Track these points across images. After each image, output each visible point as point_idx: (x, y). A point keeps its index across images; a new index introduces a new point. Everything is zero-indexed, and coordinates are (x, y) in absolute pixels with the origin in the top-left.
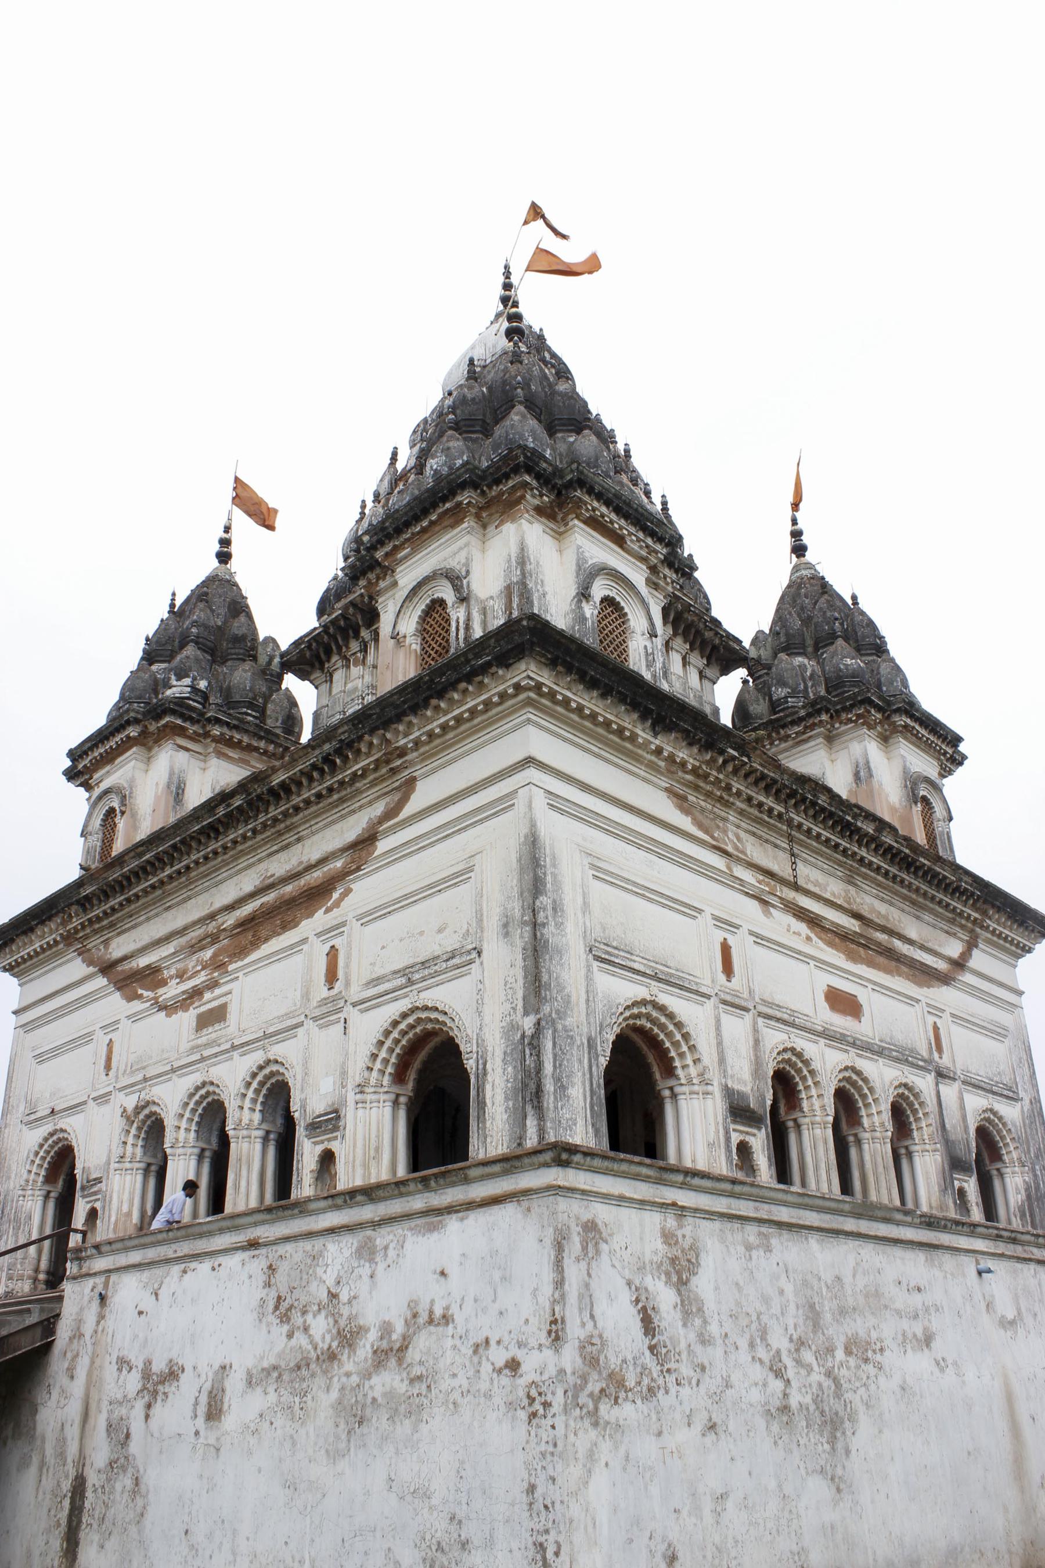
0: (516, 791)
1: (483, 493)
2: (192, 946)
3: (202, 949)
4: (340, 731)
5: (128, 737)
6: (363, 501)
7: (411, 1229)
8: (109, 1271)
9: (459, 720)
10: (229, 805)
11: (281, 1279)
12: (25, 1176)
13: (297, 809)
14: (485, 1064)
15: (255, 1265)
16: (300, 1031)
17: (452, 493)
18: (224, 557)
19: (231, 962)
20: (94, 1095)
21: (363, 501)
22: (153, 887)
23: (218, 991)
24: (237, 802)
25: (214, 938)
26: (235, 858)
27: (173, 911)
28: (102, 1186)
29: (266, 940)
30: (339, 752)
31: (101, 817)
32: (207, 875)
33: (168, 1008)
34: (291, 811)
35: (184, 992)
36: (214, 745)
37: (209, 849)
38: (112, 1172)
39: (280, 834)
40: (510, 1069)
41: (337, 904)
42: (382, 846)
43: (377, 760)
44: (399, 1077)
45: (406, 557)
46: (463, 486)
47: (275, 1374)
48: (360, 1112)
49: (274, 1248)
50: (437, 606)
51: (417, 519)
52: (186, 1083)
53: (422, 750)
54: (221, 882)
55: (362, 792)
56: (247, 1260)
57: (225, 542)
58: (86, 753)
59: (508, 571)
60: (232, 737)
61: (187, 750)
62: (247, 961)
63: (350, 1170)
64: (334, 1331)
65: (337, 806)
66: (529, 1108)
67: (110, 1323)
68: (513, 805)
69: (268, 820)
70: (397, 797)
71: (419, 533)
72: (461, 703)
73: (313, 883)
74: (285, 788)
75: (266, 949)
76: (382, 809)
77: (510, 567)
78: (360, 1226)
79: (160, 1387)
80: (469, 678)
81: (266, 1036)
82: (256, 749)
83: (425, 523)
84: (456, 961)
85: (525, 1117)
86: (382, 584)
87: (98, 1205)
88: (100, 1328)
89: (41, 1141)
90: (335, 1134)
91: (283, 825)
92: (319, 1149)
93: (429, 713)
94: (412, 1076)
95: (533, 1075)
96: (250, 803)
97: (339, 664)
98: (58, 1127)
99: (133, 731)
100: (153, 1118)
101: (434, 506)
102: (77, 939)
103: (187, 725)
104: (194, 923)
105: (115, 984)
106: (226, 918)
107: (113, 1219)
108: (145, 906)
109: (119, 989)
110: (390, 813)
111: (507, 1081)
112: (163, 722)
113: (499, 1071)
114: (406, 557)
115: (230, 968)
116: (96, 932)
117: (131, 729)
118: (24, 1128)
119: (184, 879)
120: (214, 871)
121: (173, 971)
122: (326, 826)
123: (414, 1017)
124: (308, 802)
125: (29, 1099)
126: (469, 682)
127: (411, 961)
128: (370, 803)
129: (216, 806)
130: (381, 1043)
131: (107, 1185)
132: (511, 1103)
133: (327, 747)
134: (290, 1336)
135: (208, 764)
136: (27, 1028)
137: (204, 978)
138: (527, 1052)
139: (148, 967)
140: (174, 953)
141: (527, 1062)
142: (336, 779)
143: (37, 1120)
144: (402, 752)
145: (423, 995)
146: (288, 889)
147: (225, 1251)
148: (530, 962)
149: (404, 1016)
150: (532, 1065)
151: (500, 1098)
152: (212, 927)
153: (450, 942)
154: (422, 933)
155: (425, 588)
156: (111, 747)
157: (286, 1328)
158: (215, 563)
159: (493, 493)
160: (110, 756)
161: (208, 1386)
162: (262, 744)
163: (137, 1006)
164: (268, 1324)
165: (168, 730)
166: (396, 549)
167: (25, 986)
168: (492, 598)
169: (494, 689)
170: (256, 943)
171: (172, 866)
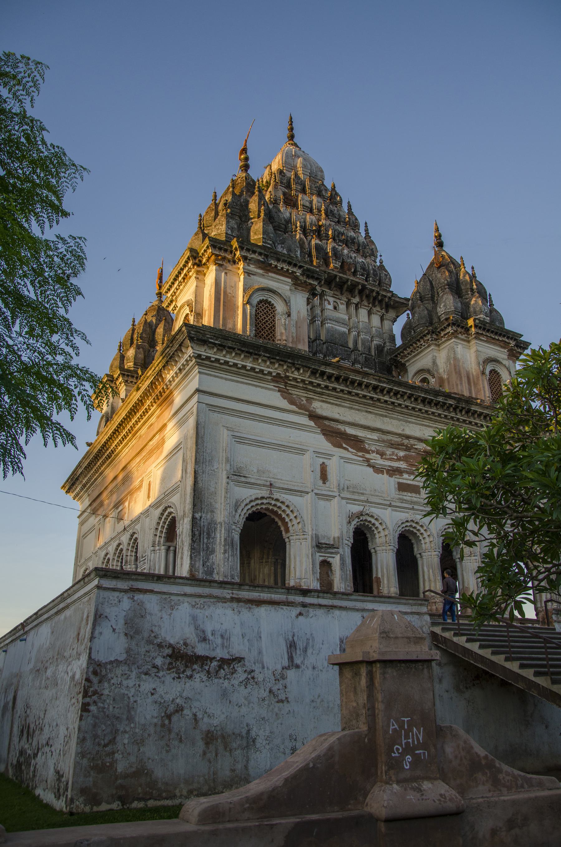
2: (392, 444)
13: (470, 423)
17: (512, 339)
20: (316, 491)
24: (451, 402)
26: (424, 418)
28: (341, 550)
33: (378, 470)
35: (390, 466)
45: (481, 340)
54: (410, 422)
86: (460, 336)
89: (253, 498)
98: (275, 497)
99: (298, 272)
101: (504, 336)
102: (286, 383)
105: (322, 430)
109: (324, 434)
114: (481, 340)
116: (306, 389)
139: (355, 436)
140: (378, 441)
143: (247, 483)
152: (406, 442)
155: (494, 363)
165: (309, 287)
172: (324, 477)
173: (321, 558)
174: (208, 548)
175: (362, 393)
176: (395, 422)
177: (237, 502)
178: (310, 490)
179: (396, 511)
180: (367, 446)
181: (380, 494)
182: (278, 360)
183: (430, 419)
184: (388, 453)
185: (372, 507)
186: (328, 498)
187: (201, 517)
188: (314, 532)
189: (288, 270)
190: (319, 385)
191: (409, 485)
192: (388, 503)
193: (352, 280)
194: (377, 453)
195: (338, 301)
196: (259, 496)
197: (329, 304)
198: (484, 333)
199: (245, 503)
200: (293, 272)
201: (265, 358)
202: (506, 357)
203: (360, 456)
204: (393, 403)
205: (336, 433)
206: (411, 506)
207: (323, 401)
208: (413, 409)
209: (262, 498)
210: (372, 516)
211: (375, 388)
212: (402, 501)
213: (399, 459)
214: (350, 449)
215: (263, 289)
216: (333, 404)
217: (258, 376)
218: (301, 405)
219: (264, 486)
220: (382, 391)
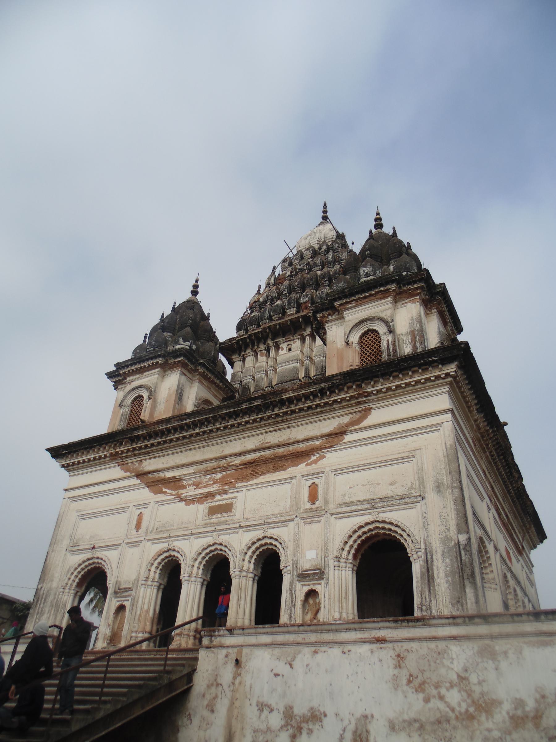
0: (442, 423)
1: (400, 288)
3: (216, 473)
4: (335, 378)
5: (157, 363)
6: (260, 285)
7: (525, 643)
8: (242, 646)
9: (408, 385)
10: (251, 404)
11: (411, 663)
12: (66, 580)
13: (293, 412)
14: (432, 556)
15: (387, 654)
16: (291, 524)
17: (387, 283)
18: (195, 293)
19: (236, 482)
20: (127, 541)
21: (260, 285)
22: (184, 437)
23: (225, 496)
25: (224, 469)
26: (243, 431)
27: (193, 451)
28: (133, 593)
29: (263, 474)
30: (329, 388)
31: (132, 399)
32: (221, 436)
33: (188, 501)
34: (289, 412)
35: (201, 494)
36: (198, 376)
37: (229, 424)
38: (139, 585)
39: (277, 423)
40: (448, 560)
41: (315, 462)
42: (348, 438)
43: (352, 396)
46: (392, 282)
47: (417, 725)
48: (336, 572)
49: (400, 644)
50: (370, 333)
51: (363, 291)
52: (199, 543)
53: (380, 395)
54: (230, 441)
55: (335, 410)
56: (375, 649)
57: (196, 286)
58: (127, 366)
59: (412, 324)
60: (207, 375)
61: (186, 375)
62: (249, 483)
63: (332, 603)
64: (469, 701)
65: (317, 415)
66: (467, 582)
67: (247, 679)
68: (439, 429)
69: (273, 414)
70: (358, 416)
71: (362, 298)
72: (411, 377)
73: (299, 450)
74: (290, 401)
75: (261, 479)
76: (348, 420)
77: (413, 322)
78: (481, 637)
79: (304, 725)
80: (420, 366)
81: (265, 523)
82: (215, 383)
83: (367, 294)
84: (407, 500)
85: (464, 587)
86: (330, 318)
87: (127, 604)
88: (237, 681)
89: (80, 562)
90: (319, 582)
91: (280, 419)
92: (306, 589)
93: (391, 378)
94: (360, 557)
95: (468, 566)
96: (264, 404)
97: (251, 353)
98: (96, 556)
99: (160, 360)
100: (170, 559)
101: (375, 287)
102: (120, 457)
103: (189, 364)
104: (211, 460)
105: (146, 484)
106: (234, 459)
107: (138, 613)
108: (173, 447)
109: (148, 487)
110: (352, 423)
111: (446, 566)
112: (178, 359)
113: (440, 560)
114: (351, 308)
115: (237, 485)
116: (135, 455)
117: (160, 359)
118: (68, 554)
119: (206, 436)
120: (227, 435)
121: (191, 482)
122: (307, 423)
123: (374, 525)
124: (301, 410)
125: (73, 537)
126: (420, 368)
127: (372, 497)
128: (340, 416)
129: (243, 403)
130: (350, 536)
131: (136, 593)
132: (450, 579)
133: (323, 385)
134: (427, 700)
135: (193, 385)
136: (73, 499)
137: (217, 489)
138: (463, 552)
140: (194, 473)
141: (463, 558)
142: (323, 401)
144: (369, 394)
145: (381, 515)
146: (281, 451)
147: (354, 642)
148: (460, 507)
149: (367, 524)
150: (467, 560)
151: (442, 575)
152: (223, 463)
153: (399, 491)
154: (378, 484)
155: (365, 323)
156: (145, 366)
157: (421, 696)
158: (190, 295)
159: (405, 288)
160: (142, 370)
161: (352, 727)
162: (218, 382)
163: (161, 497)
164: (403, 692)
165: (180, 364)
166: (347, 303)
167: (73, 477)
168: (402, 334)
169: (432, 373)
170: (254, 475)
171: (200, 428)
172: (138, 526)
173: (118, 604)
174: (42, 611)
175: (175, 437)
176: (214, 448)
177: (69, 568)
178: (120, 542)
179: (199, 537)
180: (185, 482)
181: (186, 526)
182: (106, 444)
183: (250, 429)
184: (204, 481)
185: (174, 540)
186: (135, 544)
187: (41, 588)
188: (116, 580)
189: (153, 363)
190: (140, 448)
191: (220, 506)
192: (189, 532)
193: (290, 320)
194: (194, 485)
195: (292, 342)
196: (85, 559)
197: (283, 349)
198: (348, 300)
199: (74, 567)
200: (157, 363)
201: (98, 447)
202: (390, 305)
203: (174, 495)
204: (204, 432)
205: (157, 481)
206: (213, 529)
207: (151, 458)
208: (225, 428)
209: (88, 559)
210: (174, 550)
211: (182, 428)
212: (206, 525)
213: (214, 483)
214: (168, 491)
215: (134, 389)
216: (159, 457)
217: (99, 462)
218: (133, 469)
219: (89, 549)
220: (188, 427)
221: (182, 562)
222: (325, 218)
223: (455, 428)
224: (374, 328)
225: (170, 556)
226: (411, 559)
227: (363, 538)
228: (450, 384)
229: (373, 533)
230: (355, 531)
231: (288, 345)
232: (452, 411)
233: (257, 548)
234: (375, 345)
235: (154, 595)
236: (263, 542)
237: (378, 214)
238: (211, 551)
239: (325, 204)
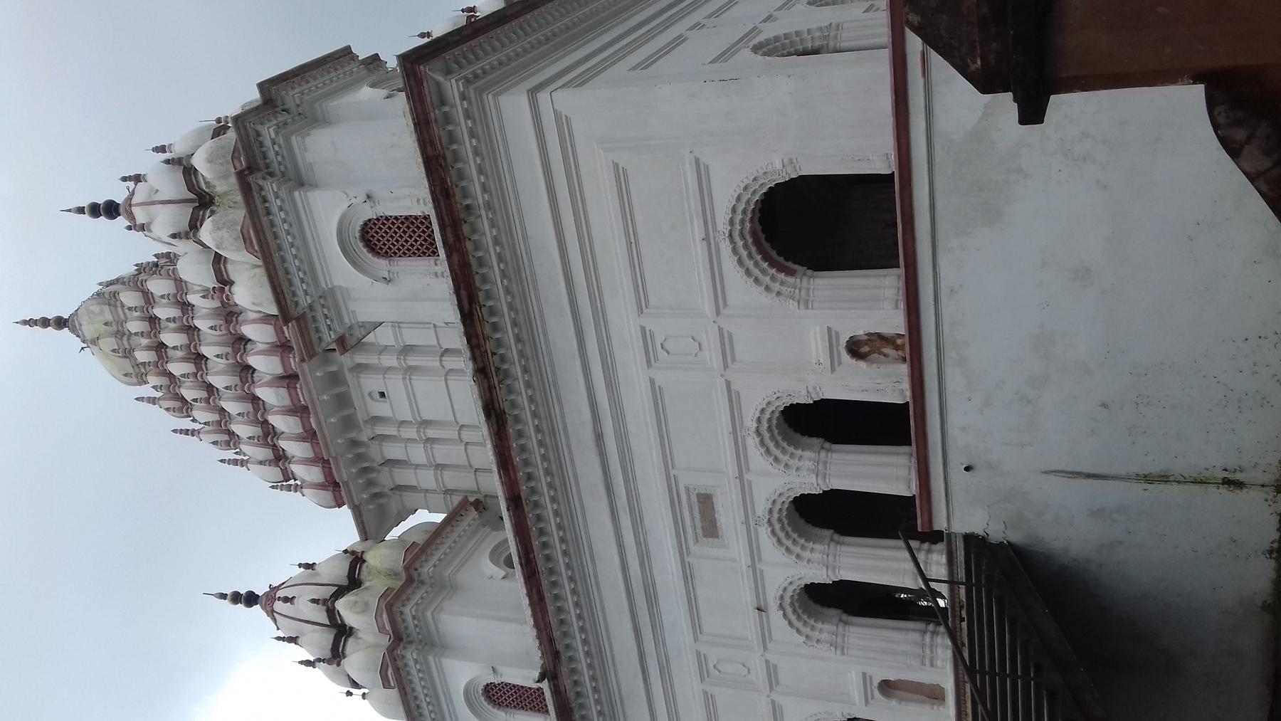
16: (733, 387)
44: (791, 273)
57: (236, 598)
94: (790, 264)
130: (757, 281)
149: (735, 251)
158: (257, 608)
191: (702, 513)
193: (318, 395)
210: (782, 597)
221: (803, 583)
222: (60, 323)
223: (561, 87)
224: (358, 228)
225: (792, 604)
226: (794, 176)
227: (759, 257)
228: (480, 91)
229: (750, 240)
230: (748, 272)
231: (372, 398)
232: (533, 92)
233: (777, 445)
234: (394, 228)
235: (860, 630)
236: (767, 435)
237: (81, 210)
238: (783, 528)
239: (25, 322)
